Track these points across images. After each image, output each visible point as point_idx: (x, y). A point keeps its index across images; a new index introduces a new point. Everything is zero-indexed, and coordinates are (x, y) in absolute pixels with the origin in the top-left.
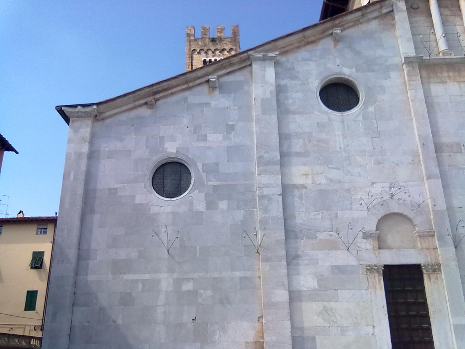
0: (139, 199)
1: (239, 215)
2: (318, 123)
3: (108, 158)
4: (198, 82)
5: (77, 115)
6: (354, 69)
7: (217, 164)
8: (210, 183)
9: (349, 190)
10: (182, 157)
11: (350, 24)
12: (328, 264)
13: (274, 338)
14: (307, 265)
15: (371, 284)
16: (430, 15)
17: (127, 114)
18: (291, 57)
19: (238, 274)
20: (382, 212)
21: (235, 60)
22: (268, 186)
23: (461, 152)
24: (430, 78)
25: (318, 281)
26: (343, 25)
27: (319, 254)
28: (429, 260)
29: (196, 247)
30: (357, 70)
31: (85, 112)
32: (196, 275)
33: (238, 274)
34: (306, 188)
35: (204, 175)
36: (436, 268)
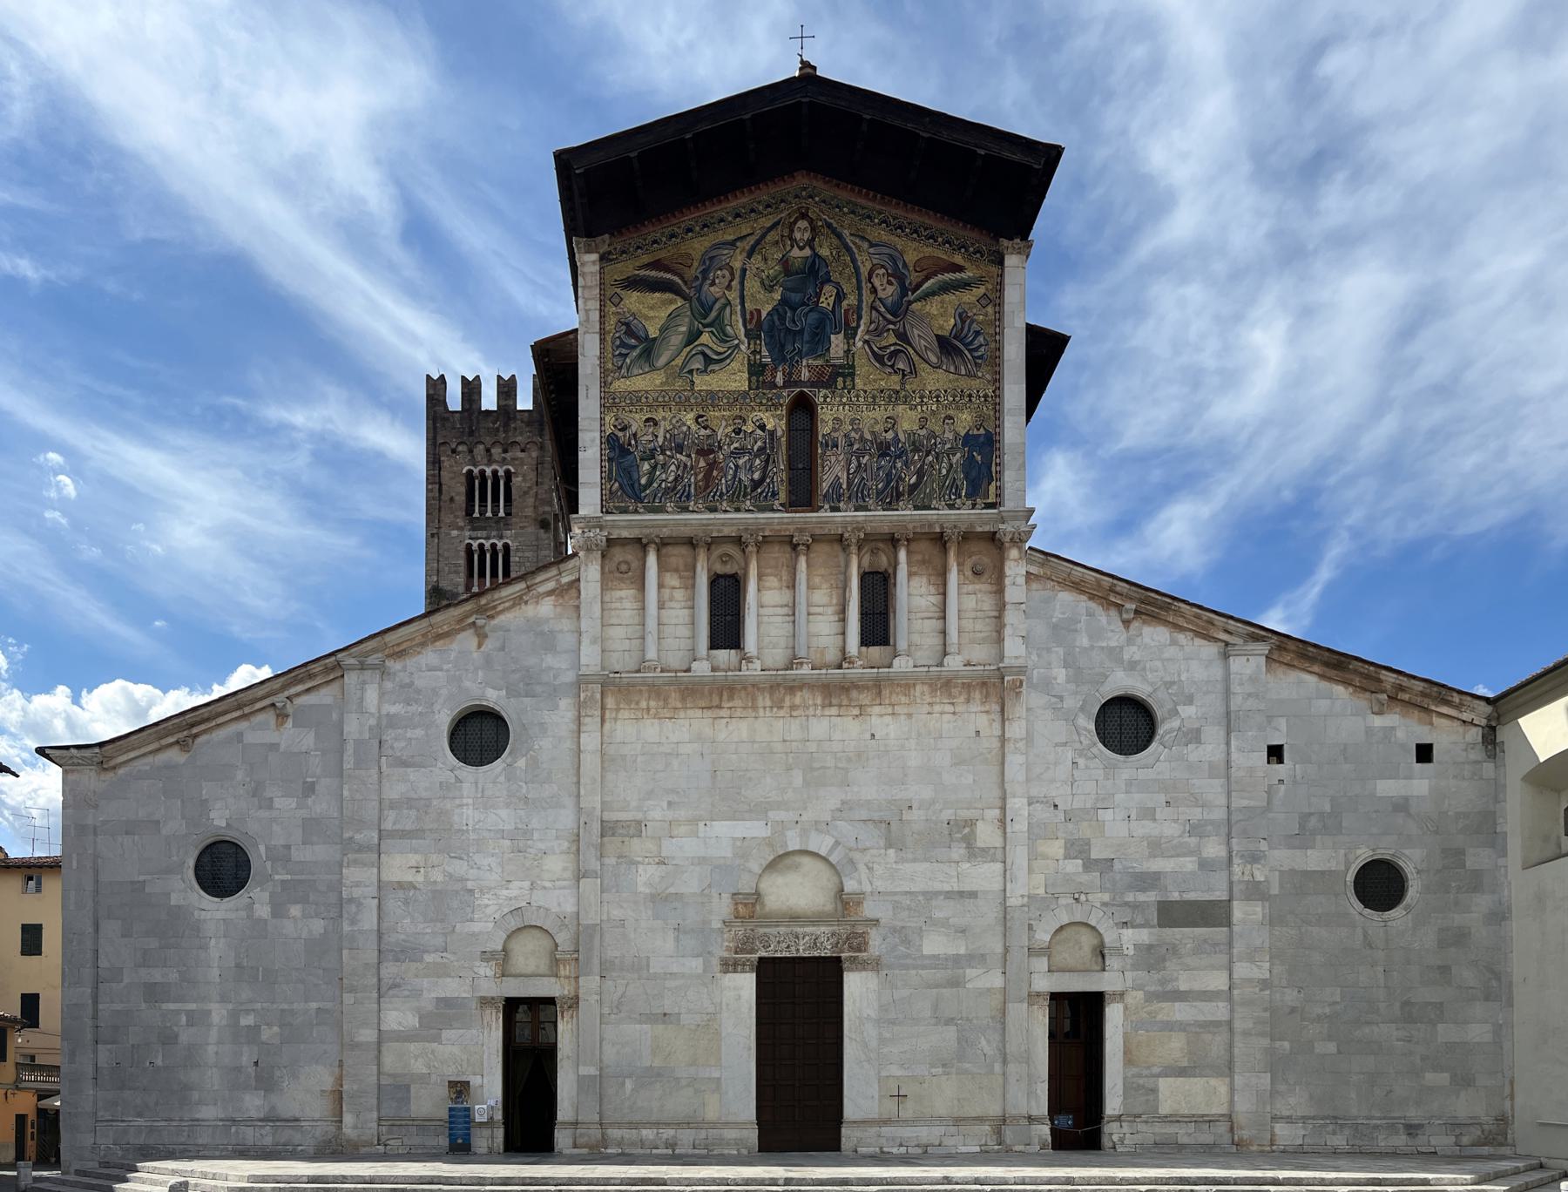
0: (175, 900)
1: (318, 926)
2: (441, 783)
3: (127, 833)
4: (258, 705)
5: (70, 762)
6: (504, 692)
7: (288, 847)
8: (277, 877)
9: (471, 891)
10: (231, 835)
11: (507, 605)
12: (434, 995)
13: (355, 1087)
14: (408, 996)
15: (485, 1022)
16: (642, 587)
17: (150, 759)
18: (411, 662)
19: (314, 1005)
20: (514, 924)
21: (317, 668)
22: (358, 884)
23: (640, 836)
24: (618, 710)
25: (420, 1018)
26: (494, 607)
27: (425, 983)
28: (566, 992)
29: (258, 970)
30: (509, 695)
31: (83, 758)
32: (258, 1006)
33: (314, 1005)
34: (415, 888)
35: (269, 864)
36: (574, 1002)
